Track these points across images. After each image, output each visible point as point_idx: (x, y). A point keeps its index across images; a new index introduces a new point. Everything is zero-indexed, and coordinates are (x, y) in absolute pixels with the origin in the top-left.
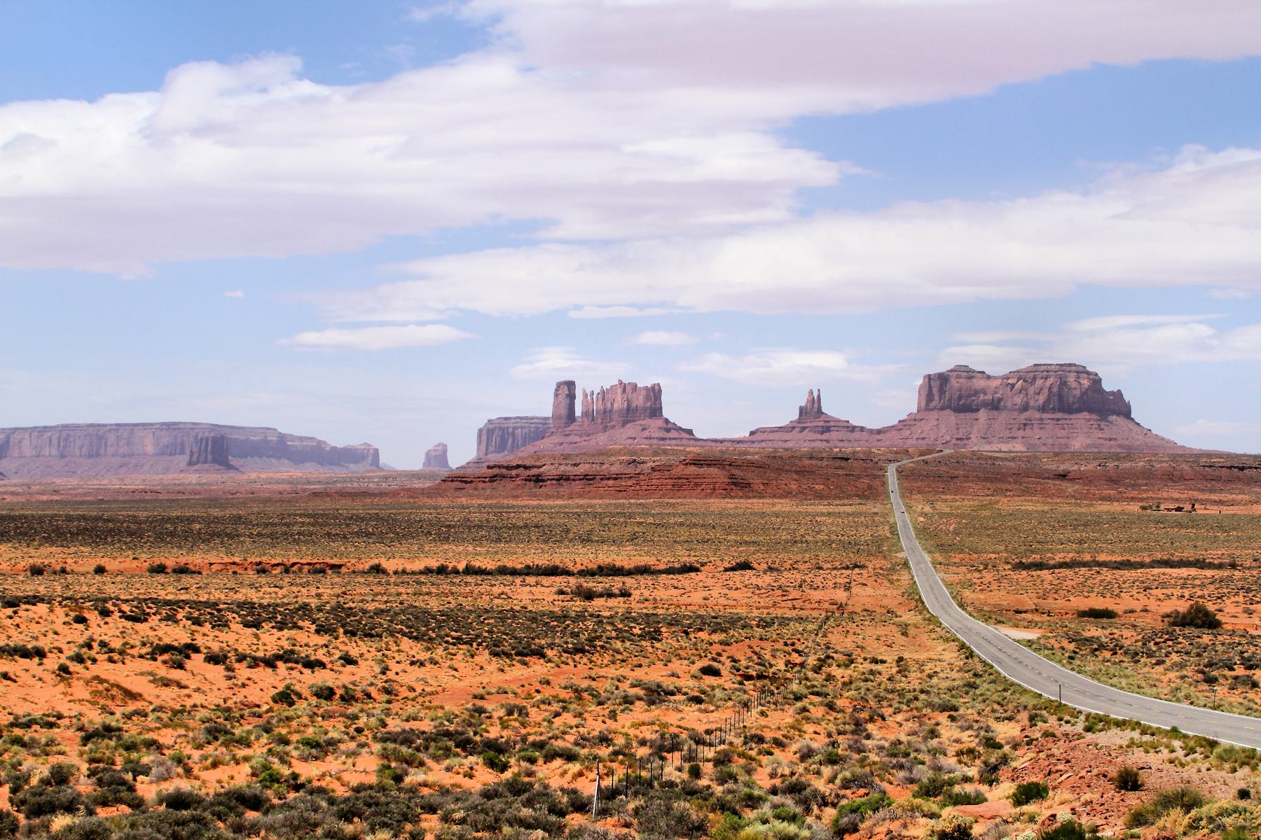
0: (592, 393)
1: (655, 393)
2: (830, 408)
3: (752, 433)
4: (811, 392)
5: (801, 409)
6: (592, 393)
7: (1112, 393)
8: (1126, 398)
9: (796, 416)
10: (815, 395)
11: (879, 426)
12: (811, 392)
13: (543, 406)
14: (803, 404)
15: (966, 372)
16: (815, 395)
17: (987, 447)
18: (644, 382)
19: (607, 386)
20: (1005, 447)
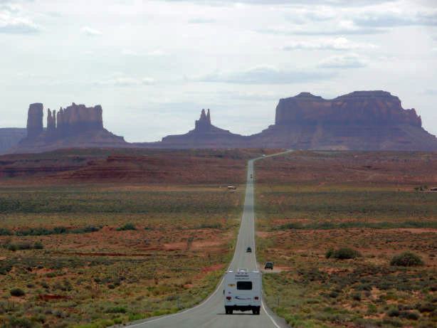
0: (54, 111)
1: (98, 110)
2: (216, 122)
3: (163, 139)
4: (203, 111)
5: (197, 123)
6: (54, 111)
7: (408, 110)
8: (418, 114)
9: (193, 127)
10: (206, 113)
11: (250, 134)
12: (203, 111)
13: (21, 122)
14: (198, 119)
15: (305, 96)
16: (206, 113)
17: (322, 148)
18: (90, 104)
19: (65, 107)
20: (334, 148)
